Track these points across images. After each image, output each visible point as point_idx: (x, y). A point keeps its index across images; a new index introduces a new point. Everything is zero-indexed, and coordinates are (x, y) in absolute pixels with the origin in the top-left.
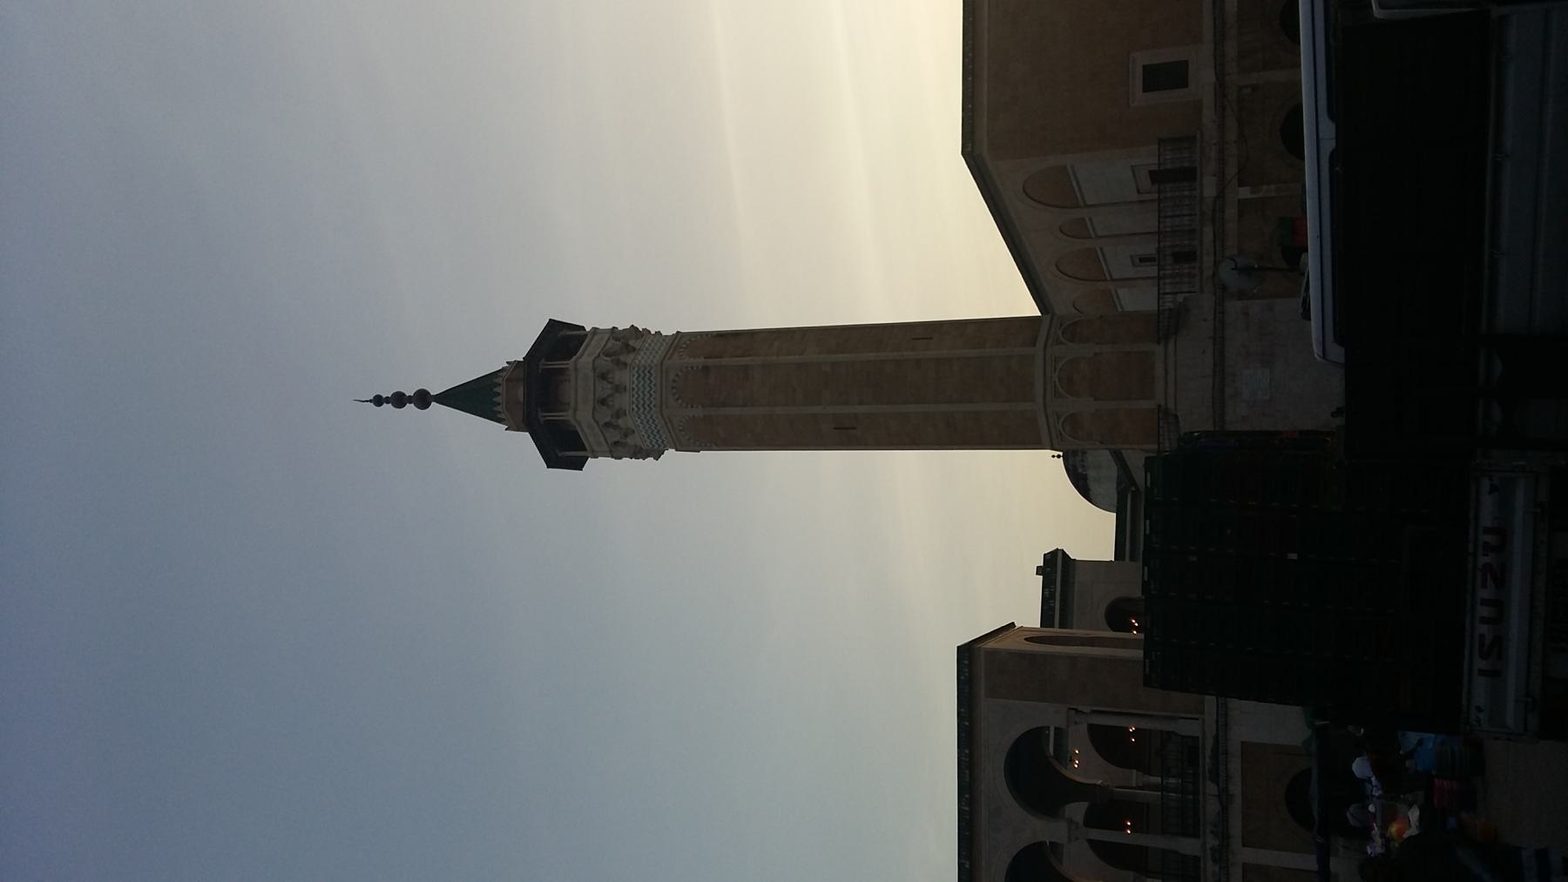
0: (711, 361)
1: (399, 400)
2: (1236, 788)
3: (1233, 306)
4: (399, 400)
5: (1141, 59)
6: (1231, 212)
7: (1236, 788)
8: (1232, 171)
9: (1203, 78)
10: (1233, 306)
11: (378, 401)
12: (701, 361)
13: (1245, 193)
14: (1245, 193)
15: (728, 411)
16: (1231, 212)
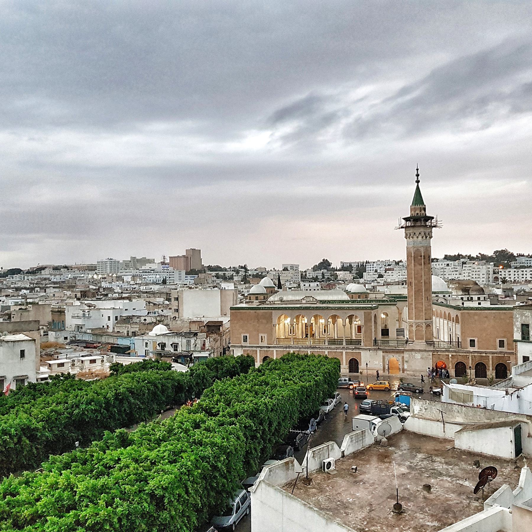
0: (423, 257)
1: (418, 175)
2: (354, 351)
3: (431, 354)
4: (418, 175)
5: (476, 340)
6: (447, 353)
7: (354, 351)
8: (454, 354)
9: (472, 349)
10: (431, 354)
11: (417, 170)
12: (423, 255)
13: (450, 356)
14: (450, 356)
15: (413, 261)
16: (447, 353)
